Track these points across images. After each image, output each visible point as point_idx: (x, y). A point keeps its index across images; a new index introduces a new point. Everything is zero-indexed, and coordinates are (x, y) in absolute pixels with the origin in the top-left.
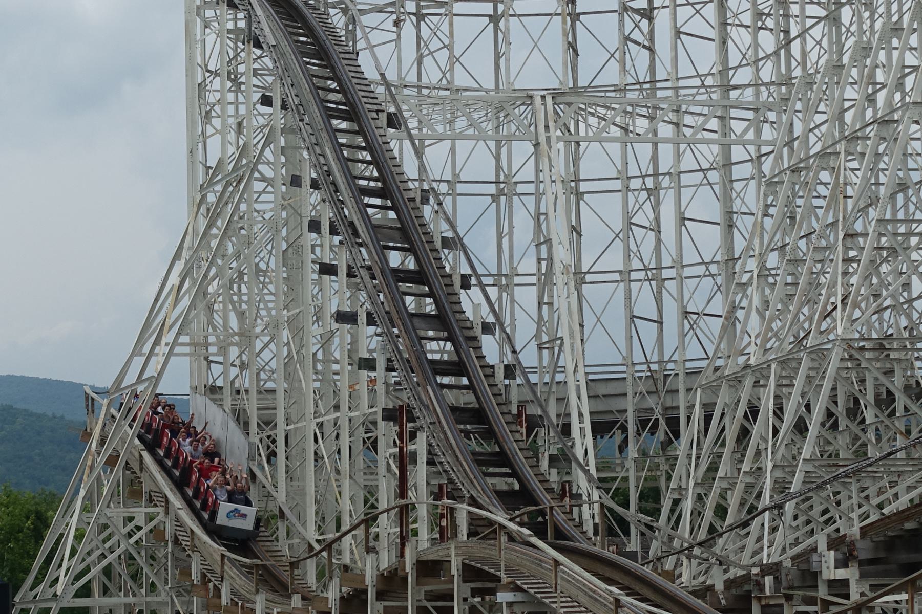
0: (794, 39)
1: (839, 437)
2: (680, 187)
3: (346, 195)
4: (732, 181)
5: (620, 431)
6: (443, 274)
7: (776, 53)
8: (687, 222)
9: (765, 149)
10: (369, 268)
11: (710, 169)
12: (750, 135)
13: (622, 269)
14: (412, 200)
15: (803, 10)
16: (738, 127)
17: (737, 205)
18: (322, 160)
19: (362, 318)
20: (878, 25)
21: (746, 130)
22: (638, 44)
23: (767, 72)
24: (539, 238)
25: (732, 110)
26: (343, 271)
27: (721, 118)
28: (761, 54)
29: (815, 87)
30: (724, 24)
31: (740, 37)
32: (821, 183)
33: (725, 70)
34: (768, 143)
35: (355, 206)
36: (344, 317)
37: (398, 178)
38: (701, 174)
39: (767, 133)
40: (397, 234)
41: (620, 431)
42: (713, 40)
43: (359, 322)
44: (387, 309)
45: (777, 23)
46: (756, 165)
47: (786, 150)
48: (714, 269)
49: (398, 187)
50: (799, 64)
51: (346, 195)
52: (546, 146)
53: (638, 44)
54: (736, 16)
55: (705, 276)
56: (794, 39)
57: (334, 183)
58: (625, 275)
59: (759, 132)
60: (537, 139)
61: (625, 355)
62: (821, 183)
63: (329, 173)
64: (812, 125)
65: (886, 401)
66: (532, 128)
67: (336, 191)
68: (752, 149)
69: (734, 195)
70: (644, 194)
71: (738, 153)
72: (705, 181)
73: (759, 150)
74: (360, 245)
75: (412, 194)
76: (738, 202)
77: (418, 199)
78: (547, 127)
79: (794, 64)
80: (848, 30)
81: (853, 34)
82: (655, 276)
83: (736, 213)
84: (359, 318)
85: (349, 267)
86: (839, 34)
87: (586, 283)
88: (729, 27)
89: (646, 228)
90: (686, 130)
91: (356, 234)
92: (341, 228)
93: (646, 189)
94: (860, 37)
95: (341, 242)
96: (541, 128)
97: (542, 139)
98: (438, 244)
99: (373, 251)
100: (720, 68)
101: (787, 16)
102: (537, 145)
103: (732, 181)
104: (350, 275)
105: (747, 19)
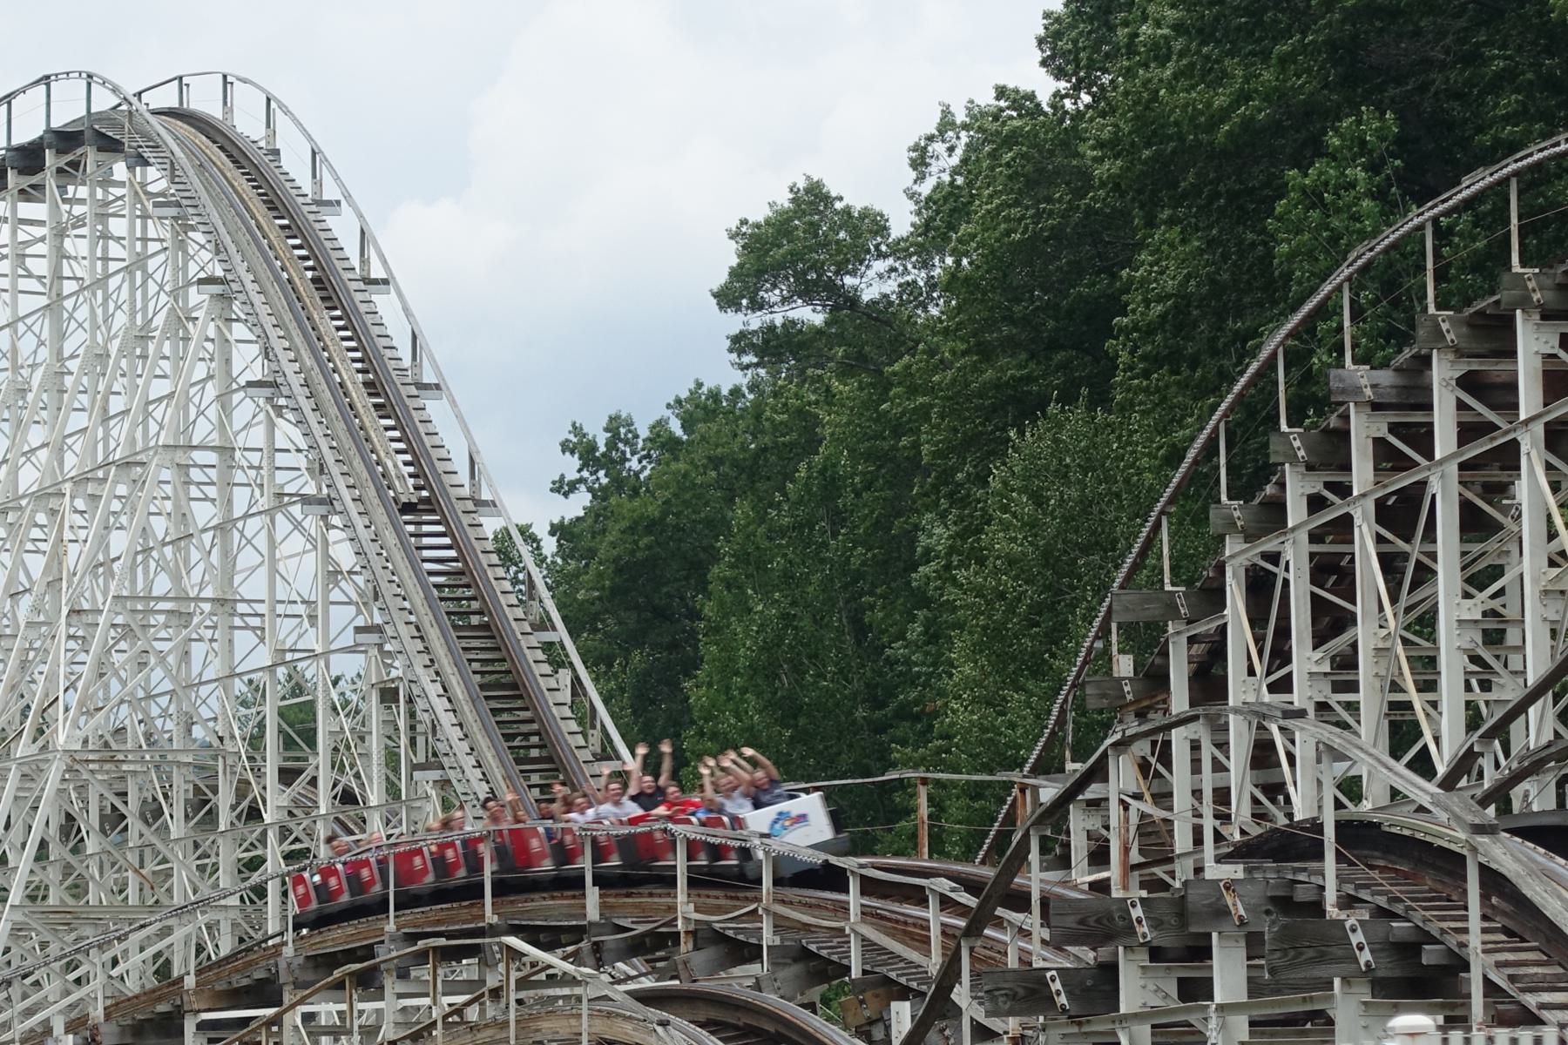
1: (49, 869)
15: (14, 284)
20: (120, 319)
29: (30, 397)
32: (36, 525)
62: (36, 525)
64: (26, 448)
65: (113, 820)
81: (80, 325)
94: (93, 337)
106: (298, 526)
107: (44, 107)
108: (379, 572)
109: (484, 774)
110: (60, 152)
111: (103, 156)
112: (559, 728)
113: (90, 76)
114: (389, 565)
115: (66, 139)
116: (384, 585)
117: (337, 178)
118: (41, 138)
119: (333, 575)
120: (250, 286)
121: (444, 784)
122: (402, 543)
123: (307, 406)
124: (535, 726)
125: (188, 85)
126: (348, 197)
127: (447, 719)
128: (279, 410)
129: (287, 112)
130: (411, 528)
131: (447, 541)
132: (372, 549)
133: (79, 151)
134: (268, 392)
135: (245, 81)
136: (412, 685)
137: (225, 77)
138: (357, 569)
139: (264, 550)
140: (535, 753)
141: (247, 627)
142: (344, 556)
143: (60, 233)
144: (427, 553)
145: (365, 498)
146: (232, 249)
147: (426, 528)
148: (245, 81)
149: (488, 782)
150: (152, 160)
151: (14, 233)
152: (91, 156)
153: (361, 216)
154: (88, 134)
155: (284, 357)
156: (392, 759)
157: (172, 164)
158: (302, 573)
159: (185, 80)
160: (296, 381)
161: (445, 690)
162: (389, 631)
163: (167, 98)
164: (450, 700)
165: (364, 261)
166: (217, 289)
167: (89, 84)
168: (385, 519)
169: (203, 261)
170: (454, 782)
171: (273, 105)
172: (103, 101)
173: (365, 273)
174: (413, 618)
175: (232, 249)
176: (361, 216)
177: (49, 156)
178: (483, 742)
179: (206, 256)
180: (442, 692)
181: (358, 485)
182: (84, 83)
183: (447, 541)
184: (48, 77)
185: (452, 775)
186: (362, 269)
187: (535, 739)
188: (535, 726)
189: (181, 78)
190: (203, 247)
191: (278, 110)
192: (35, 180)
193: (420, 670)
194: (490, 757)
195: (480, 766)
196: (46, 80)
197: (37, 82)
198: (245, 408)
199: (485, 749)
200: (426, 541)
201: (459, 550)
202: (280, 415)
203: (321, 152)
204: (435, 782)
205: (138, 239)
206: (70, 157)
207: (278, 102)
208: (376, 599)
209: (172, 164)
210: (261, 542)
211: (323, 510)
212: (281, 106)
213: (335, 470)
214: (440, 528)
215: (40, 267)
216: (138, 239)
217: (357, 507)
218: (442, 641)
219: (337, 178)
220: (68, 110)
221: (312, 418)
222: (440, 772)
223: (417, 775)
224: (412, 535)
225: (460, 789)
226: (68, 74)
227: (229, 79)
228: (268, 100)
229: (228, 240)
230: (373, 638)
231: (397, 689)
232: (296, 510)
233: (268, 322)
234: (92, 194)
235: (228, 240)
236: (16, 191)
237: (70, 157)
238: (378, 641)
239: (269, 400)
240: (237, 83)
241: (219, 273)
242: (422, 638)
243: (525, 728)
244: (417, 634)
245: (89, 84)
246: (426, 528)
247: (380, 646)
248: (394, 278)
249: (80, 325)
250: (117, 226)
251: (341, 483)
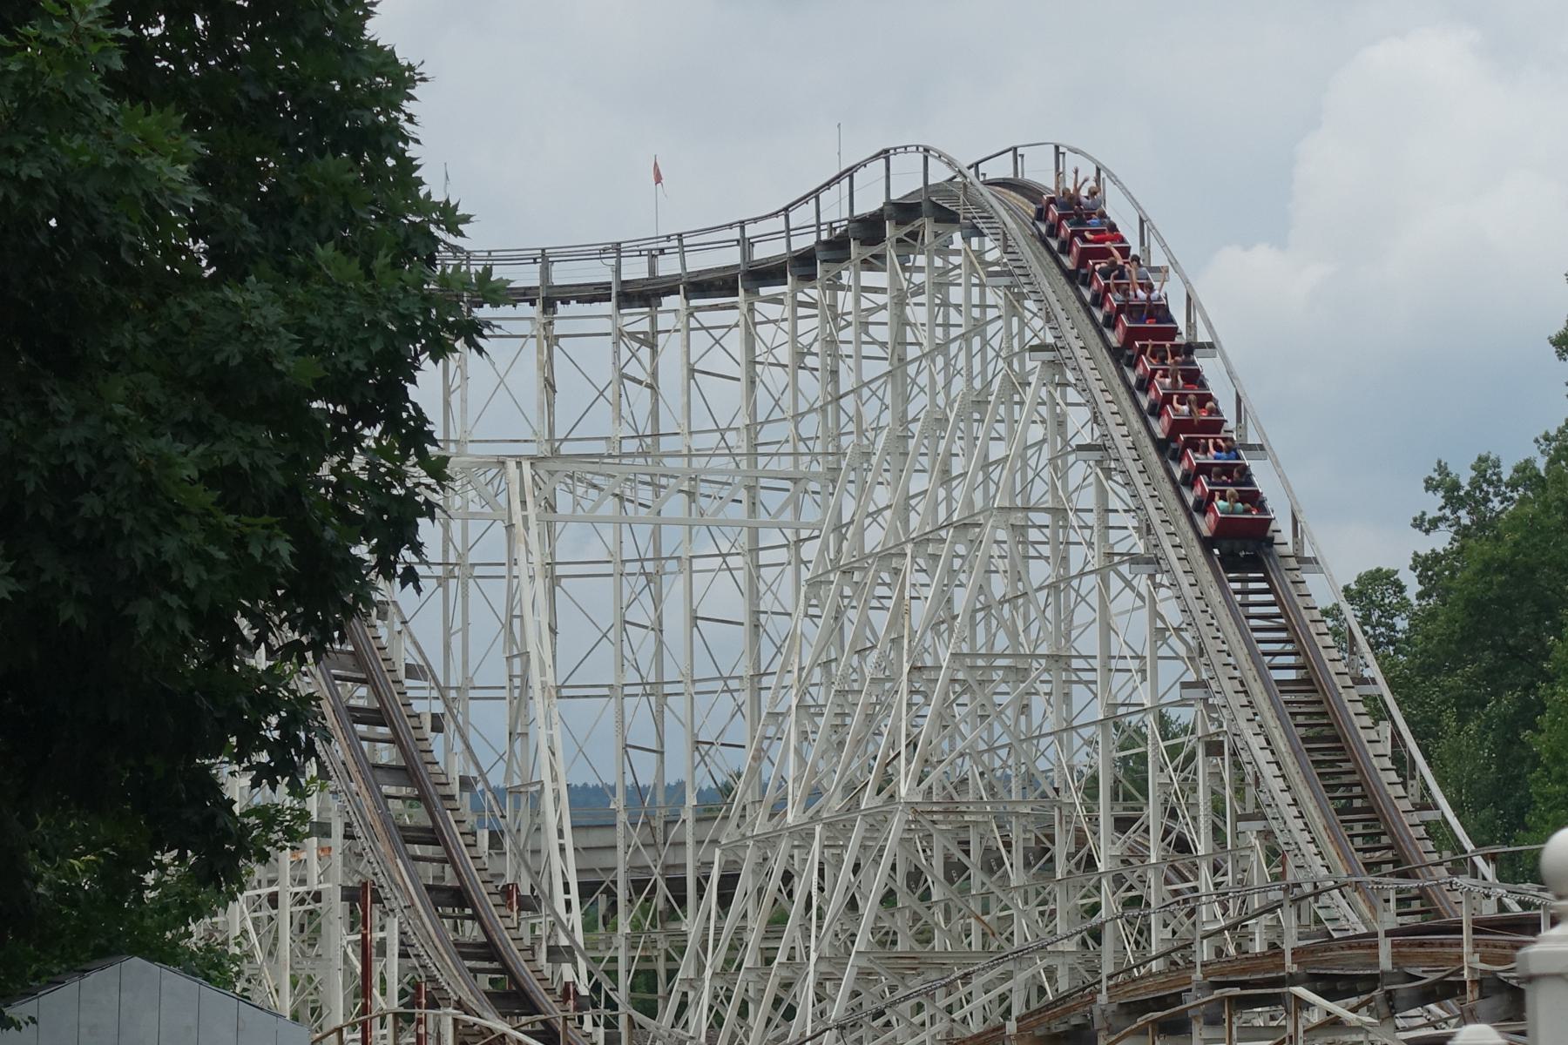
0: (846, 394)
2: (691, 572)
4: (759, 567)
7: (823, 409)
8: (699, 622)
9: (804, 534)
11: (729, 554)
12: (788, 516)
15: (858, 350)
16: (772, 500)
17: (766, 603)
21: (782, 509)
22: (640, 383)
23: (810, 426)
24: (511, 650)
25: (762, 480)
27: (749, 488)
28: (803, 407)
30: (752, 363)
31: (774, 378)
33: (753, 427)
34: (807, 526)
38: (721, 559)
39: (810, 513)
42: (738, 380)
45: (824, 364)
46: (793, 552)
47: (832, 536)
48: (733, 684)
50: (851, 419)
52: (522, 529)
53: (640, 383)
54: (770, 350)
55: (723, 691)
56: (846, 394)
59: (798, 511)
60: (510, 518)
66: (502, 499)
68: (788, 532)
69: (762, 588)
70: (643, 580)
71: (770, 537)
72: (724, 566)
73: (797, 532)
76: (769, 597)
78: (524, 503)
79: (844, 419)
80: (914, 382)
82: (655, 690)
83: (766, 612)
86: (904, 384)
88: (759, 368)
89: (646, 627)
90: (703, 502)
93: (645, 574)
96: (516, 505)
97: (517, 520)
100: (748, 422)
101: (836, 357)
102: (510, 527)
103: (759, 567)
105: (784, 354)
106: (1128, 584)
107: (884, 180)
108: (1204, 629)
109: (1306, 824)
110: (900, 223)
111: (940, 228)
112: (1379, 778)
113: (926, 150)
114: (1214, 622)
115: (904, 211)
116: (1209, 642)
117: (1164, 246)
118: (881, 210)
119: (1160, 634)
120: (1079, 353)
121: (1267, 834)
122: (1226, 601)
123: (1134, 469)
124: (1357, 777)
125: (1022, 156)
126: (1174, 263)
127: (1269, 771)
128: (1108, 472)
129: (1116, 182)
130: (1237, 586)
131: (1270, 597)
132: (1196, 607)
133: (918, 222)
134: (1097, 455)
135: (1075, 151)
136: (1237, 738)
137: (1057, 148)
138: (1184, 626)
139: (1095, 603)
140: (1357, 803)
141: (1080, 682)
142: (1172, 613)
143: (900, 301)
144: (1253, 610)
145: (1190, 557)
146: (1062, 316)
147: (1252, 586)
148: (1075, 151)
149: (1310, 832)
150: (986, 231)
151: (857, 301)
152: (928, 227)
153: (1186, 282)
154: (925, 207)
155: (1111, 421)
156: (1218, 809)
157: (1005, 234)
158: (1134, 630)
159: (1020, 151)
160: (1123, 444)
161: (1269, 743)
162: (1214, 686)
163: (1001, 169)
164: (1273, 753)
165: (1191, 326)
166: (1048, 356)
167: (926, 158)
168: (1210, 577)
169: (1037, 329)
170: (1277, 832)
171: (1103, 174)
172: (939, 173)
173: (1192, 338)
174: (1237, 674)
175: (1062, 316)
176: (1186, 282)
177: (889, 227)
178: (1305, 794)
179: (1038, 323)
180: (1265, 745)
181: (1184, 545)
182: (921, 157)
183: (1270, 597)
184: (887, 151)
185: (1274, 825)
186: (1188, 334)
187: (1357, 790)
188: (1357, 777)
189: (1015, 149)
190: (1035, 315)
191: (1107, 180)
192: (876, 250)
193: (1243, 724)
194: (1311, 807)
195: (1302, 817)
196: (885, 154)
197: (877, 156)
198: (1079, 470)
199: (1307, 800)
200: (1252, 598)
201: (1282, 607)
202: (1109, 478)
203: (1148, 220)
204: (1258, 832)
205: (975, 306)
206: (908, 229)
207: (1107, 171)
208: (1201, 655)
209: (1005, 234)
210: (1094, 599)
211: (1150, 568)
212: (1110, 175)
213: (1161, 530)
214: (1264, 585)
215: (882, 334)
216: (975, 306)
217: (1182, 566)
218: (1265, 694)
219: (1164, 246)
220: (906, 184)
221: (1139, 480)
222: (1264, 822)
223: (1242, 826)
224: (1237, 592)
225: (1281, 840)
226: (906, 148)
227: (1062, 150)
228: (1098, 170)
229: (1057, 308)
230: (1199, 693)
231: (1222, 742)
232: (1124, 569)
233: (1096, 387)
234: (931, 262)
235: (1057, 308)
236: (858, 262)
237: (908, 229)
238: (1204, 696)
239: (1098, 462)
240: (1068, 154)
241: (1050, 340)
242: (1245, 692)
243: (1346, 779)
244: (1241, 689)
245: (926, 158)
246: (1252, 586)
247: (1206, 700)
248: (1219, 342)
249: (922, 390)
250: (956, 295)
251: (1167, 543)
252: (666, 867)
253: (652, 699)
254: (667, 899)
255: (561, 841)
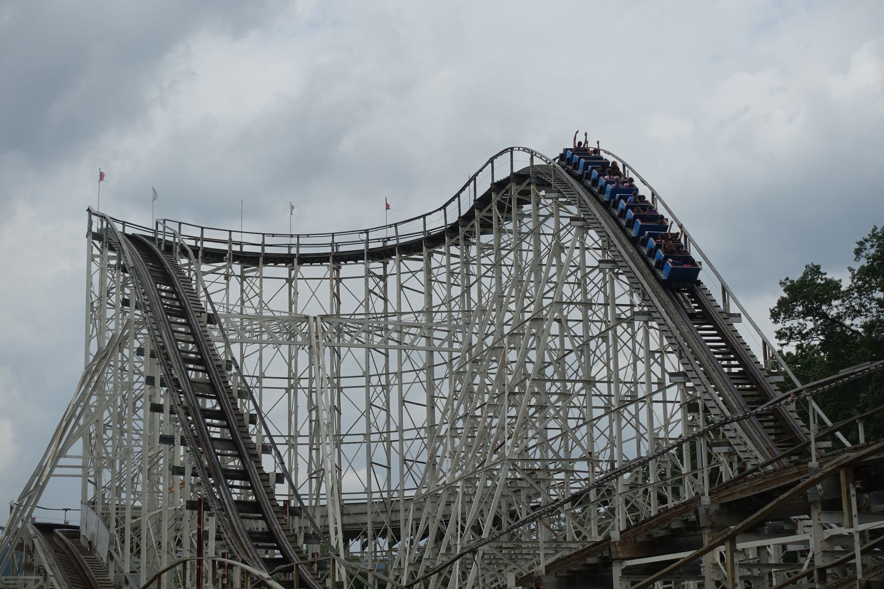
3: (173, 361)
5: (363, 536)
6: (237, 413)
10: (185, 408)
13: (365, 433)
14: (220, 366)
18: (159, 339)
19: (178, 440)
26: (167, 409)
35: (179, 367)
36: (167, 440)
37: (211, 353)
40: (207, 388)
41: (363, 536)
43: (176, 443)
44: (196, 434)
49: (210, 357)
51: (173, 361)
52: (316, 349)
57: (167, 354)
58: (367, 435)
61: (366, 487)
63: (164, 348)
67: (168, 359)
74: (181, 393)
75: (220, 363)
77: (224, 366)
84: (175, 440)
85: (171, 406)
87: (343, 443)
91: (179, 386)
92: (167, 381)
95: (167, 391)
97: (314, 344)
98: (235, 394)
99: (189, 396)
104: (172, 412)
252: (392, 522)
253: (385, 443)
254: (393, 537)
255: (333, 498)
